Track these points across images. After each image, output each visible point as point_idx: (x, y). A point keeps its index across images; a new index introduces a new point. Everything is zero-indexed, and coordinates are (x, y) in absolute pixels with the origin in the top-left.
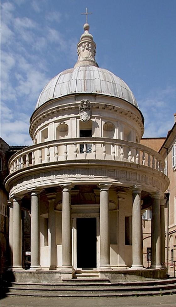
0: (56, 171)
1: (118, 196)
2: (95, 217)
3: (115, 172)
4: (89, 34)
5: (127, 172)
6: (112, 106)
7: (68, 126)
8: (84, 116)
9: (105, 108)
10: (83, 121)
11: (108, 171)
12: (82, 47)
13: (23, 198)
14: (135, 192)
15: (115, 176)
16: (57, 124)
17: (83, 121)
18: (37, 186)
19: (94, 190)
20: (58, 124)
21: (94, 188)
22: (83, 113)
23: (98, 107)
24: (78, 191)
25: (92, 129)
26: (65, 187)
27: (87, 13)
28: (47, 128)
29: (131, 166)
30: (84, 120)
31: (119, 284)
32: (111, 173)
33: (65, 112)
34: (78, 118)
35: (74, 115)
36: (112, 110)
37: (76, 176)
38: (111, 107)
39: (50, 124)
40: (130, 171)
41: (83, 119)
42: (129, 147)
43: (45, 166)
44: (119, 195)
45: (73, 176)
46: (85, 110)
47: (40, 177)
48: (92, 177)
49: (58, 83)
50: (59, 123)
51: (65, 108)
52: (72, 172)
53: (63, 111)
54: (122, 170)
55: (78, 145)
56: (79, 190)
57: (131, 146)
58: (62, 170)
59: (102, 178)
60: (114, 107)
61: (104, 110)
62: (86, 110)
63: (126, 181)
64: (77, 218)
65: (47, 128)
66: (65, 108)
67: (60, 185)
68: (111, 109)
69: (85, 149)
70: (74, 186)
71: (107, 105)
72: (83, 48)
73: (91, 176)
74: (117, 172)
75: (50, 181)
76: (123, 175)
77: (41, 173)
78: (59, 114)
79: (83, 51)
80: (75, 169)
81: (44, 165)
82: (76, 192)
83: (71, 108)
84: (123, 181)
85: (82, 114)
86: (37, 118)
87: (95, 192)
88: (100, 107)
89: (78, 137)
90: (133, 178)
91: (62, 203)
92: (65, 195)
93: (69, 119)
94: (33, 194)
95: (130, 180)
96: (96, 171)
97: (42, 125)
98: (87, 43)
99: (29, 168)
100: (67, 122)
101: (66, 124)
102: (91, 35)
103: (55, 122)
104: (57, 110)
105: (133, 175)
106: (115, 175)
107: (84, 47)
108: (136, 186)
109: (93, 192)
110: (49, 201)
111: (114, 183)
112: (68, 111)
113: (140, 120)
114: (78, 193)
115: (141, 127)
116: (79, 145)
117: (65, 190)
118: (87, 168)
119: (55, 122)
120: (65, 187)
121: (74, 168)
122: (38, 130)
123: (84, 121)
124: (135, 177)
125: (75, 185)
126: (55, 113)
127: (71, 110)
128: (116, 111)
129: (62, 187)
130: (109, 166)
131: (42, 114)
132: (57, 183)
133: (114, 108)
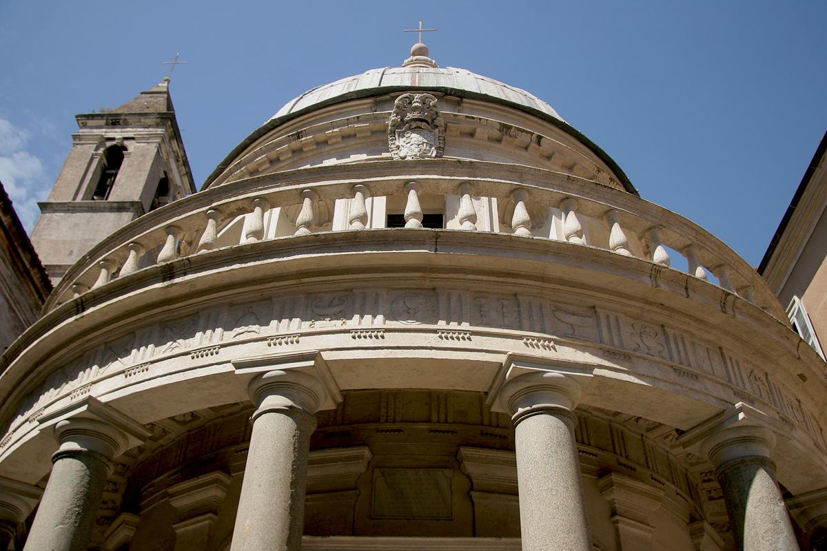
0: (231, 305)
1: (611, 503)
3: (598, 318)
5: (670, 332)
6: (532, 134)
9: (499, 141)
11: (558, 309)
14: (739, 451)
15: (601, 341)
19: (465, 451)
21: (471, 424)
22: (404, 139)
23: (472, 135)
24: (357, 458)
25: (444, 209)
26: (275, 386)
27: (421, 29)
29: (688, 296)
32: (573, 320)
33: (328, 148)
35: (362, 157)
36: (530, 149)
37: (354, 322)
38: (525, 139)
40: (686, 331)
42: (650, 228)
43: (172, 277)
44: (619, 497)
45: (337, 324)
46: (413, 130)
47: (134, 351)
48: (454, 331)
52: (330, 305)
54: (637, 318)
56: (366, 452)
57: (660, 226)
58: (270, 299)
59: (521, 342)
60: (540, 138)
61: (498, 146)
63: (673, 376)
68: (526, 148)
70: (340, 400)
71: (510, 127)
73: (454, 325)
74: (612, 321)
75: (186, 362)
77: (143, 327)
78: (301, 159)
80: (351, 290)
81: (168, 272)
82: (349, 459)
84: (657, 374)
87: (470, 467)
88: (478, 130)
90: (706, 366)
95: (695, 377)
96: (483, 301)
102: (434, 61)
104: (295, 144)
105: (702, 354)
106: (600, 332)
108: (740, 410)
109: (453, 461)
110: (181, 529)
112: (336, 146)
114: (361, 468)
118: (428, 284)
120: (275, 386)
121: (346, 285)
124: (719, 368)
125: (346, 394)
126: (284, 161)
127: (351, 142)
130: (562, 282)
133: (539, 143)
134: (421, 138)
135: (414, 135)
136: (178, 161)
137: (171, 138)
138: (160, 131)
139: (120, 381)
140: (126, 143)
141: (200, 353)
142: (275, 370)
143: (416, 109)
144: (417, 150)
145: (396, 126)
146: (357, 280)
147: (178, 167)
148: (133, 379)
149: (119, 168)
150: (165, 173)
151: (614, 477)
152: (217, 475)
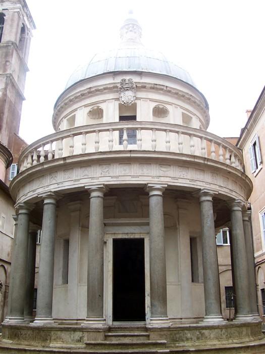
2: (142, 237)
7: (102, 110)
13: (34, 209)
18: (53, 190)
28: (75, 115)
31: (184, 350)
32: (164, 169)
34: (118, 99)
39: (78, 109)
41: (123, 101)
49: (92, 62)
53: (98, 91)
55: (117, 133)
64: (116, 241)
65: (75, 115)
67: (86, 188)
69: (125, 137)
72: (127, 30)
76: (183, 173)
79: (127, 33)
86: (62, 103)
89: (117, 120)
91: (89, 216)
92: (96, 203)
93: (104, 101)
97: (69, 110)
98: (131, 25)
99: (43, 164)
100: (102, 106)
103: (86, 106)
107: (127, 29)
111: (170, 185)
113: (203, 105)
115: (205, 115)
116: (118, 132)
119: (86, 106)
122: (62, 118)
125: (111, 189)
128: (169, 92)
129: (89, 191)
131: (69, 97)
132: (83, 185)
136: (27, 16)
137: (23, 7)
138: (19, 5)
139: (56, 186)
140: (4, 12)
142: (94, 187)
143: (126, 83)
145: (121, 88)
147: (28, 19)
149: (3, 24)
150: (23, 24)
151: (178, 199)
152: (79, 202)
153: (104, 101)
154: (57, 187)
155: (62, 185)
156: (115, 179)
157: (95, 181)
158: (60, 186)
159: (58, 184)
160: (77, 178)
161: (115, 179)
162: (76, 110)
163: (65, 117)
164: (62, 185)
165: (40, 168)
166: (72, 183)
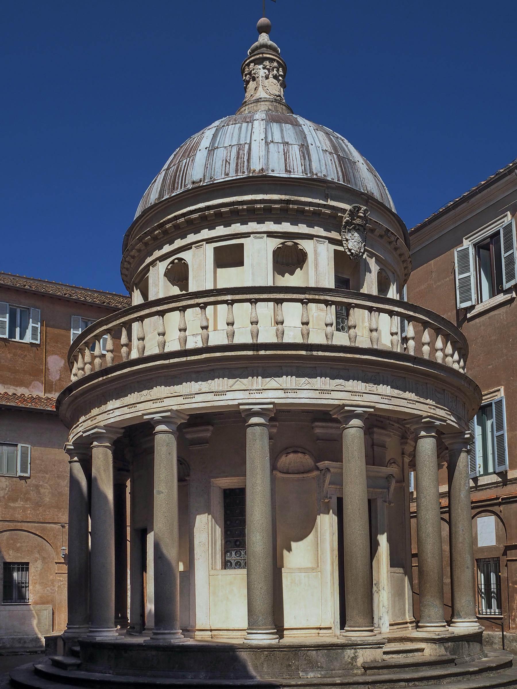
4: (270, 43)
8: (353, 242)
10: (349, 253)
12: (261, 66)
16: (275, 243)
17: (349, 253)
20: (275, 243)
26: (358, 416)
30: (352, 251)
34: (339, 243)
41: (350, 250)
50: (282, 241)
51: (307, 208)
62: (358, 229)
66: (307, 208)
80: (379, 373)
83: (303, 211)
85: (349, 236)
93: (310, 237)
94: (254, 420)
101: (300, 247)
103: (271, 234)
117: (355, 422)
119: (271, 234)
120: (358, 416)
123: (352, 253)
134: (359, 238)
135: (356, 234)
139: (281, 394)
141: (322, 391)
142: (359, 410)
144: (357, 247)
146: (382, 370)
148: (289, 395)
153: (310, 237)
154: (284, 395)
155: (294, 395)
156: (386, 401)
157: (357, 398)
158: (289, 395)
159: (285, 390)
160: (323, 387)
161: (386, 401)
162: (246, 235)
163: (209, 241)
164: (294, 395)
165: (250, 353)
166: (316, 394)
